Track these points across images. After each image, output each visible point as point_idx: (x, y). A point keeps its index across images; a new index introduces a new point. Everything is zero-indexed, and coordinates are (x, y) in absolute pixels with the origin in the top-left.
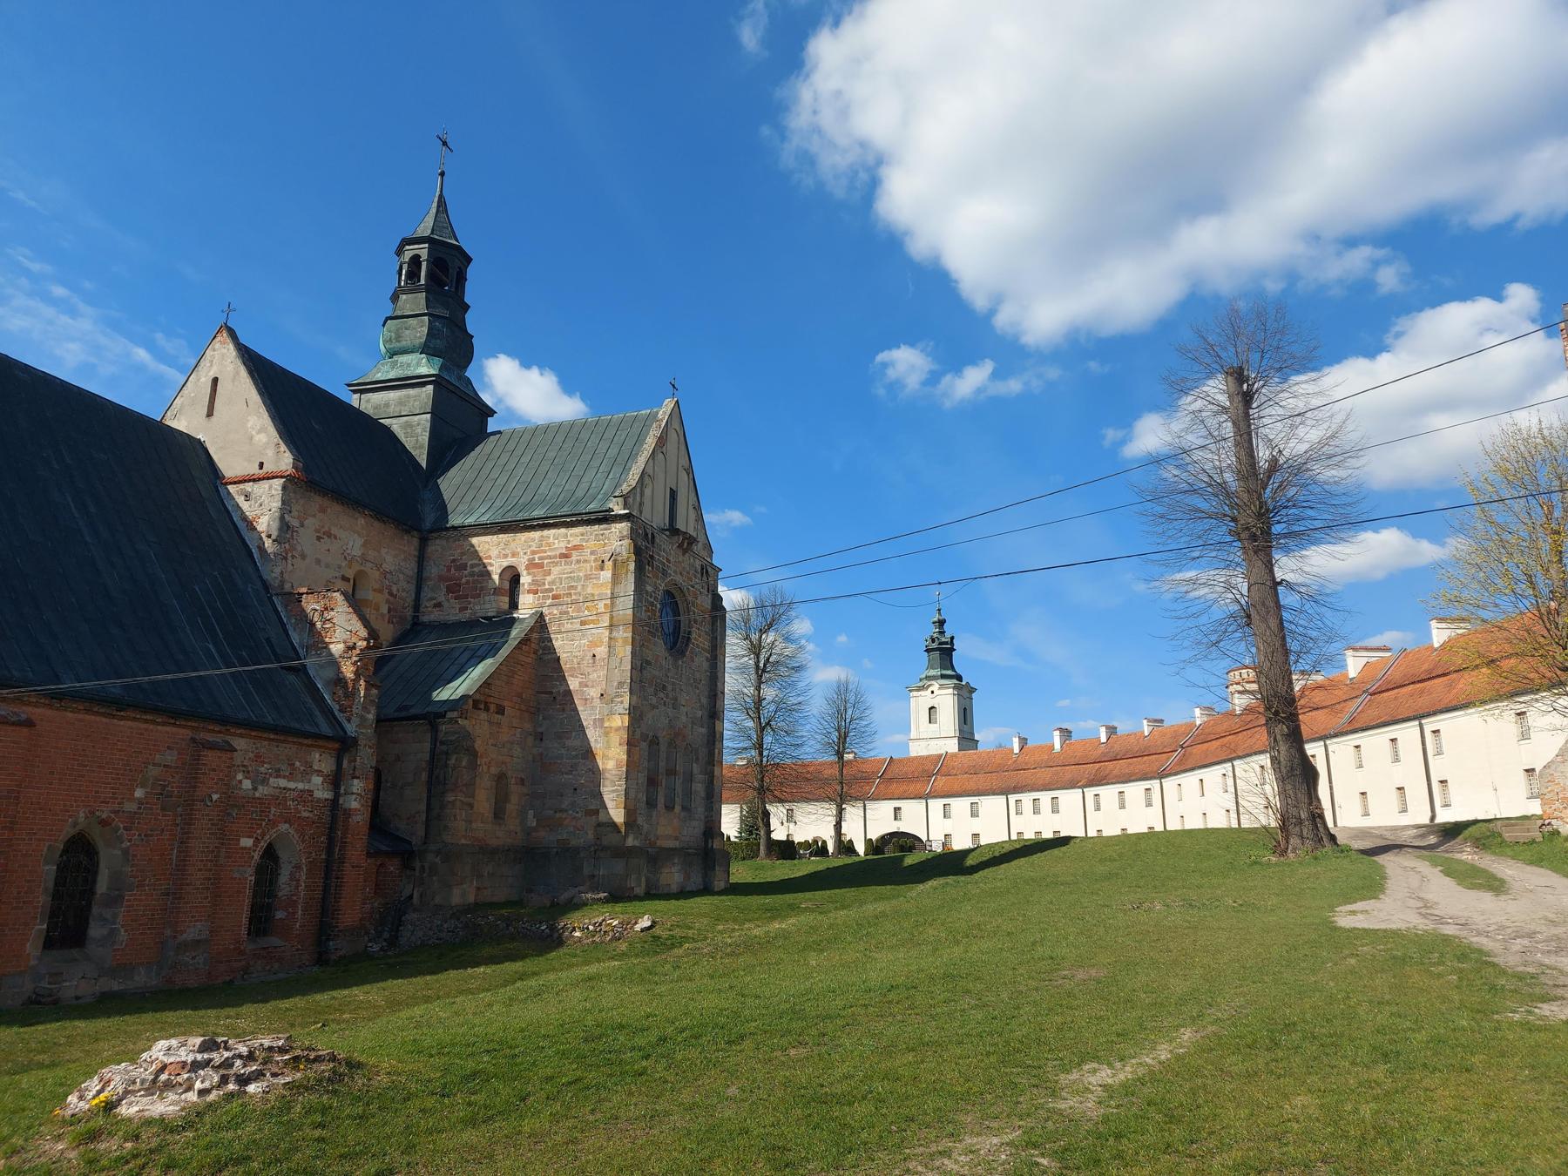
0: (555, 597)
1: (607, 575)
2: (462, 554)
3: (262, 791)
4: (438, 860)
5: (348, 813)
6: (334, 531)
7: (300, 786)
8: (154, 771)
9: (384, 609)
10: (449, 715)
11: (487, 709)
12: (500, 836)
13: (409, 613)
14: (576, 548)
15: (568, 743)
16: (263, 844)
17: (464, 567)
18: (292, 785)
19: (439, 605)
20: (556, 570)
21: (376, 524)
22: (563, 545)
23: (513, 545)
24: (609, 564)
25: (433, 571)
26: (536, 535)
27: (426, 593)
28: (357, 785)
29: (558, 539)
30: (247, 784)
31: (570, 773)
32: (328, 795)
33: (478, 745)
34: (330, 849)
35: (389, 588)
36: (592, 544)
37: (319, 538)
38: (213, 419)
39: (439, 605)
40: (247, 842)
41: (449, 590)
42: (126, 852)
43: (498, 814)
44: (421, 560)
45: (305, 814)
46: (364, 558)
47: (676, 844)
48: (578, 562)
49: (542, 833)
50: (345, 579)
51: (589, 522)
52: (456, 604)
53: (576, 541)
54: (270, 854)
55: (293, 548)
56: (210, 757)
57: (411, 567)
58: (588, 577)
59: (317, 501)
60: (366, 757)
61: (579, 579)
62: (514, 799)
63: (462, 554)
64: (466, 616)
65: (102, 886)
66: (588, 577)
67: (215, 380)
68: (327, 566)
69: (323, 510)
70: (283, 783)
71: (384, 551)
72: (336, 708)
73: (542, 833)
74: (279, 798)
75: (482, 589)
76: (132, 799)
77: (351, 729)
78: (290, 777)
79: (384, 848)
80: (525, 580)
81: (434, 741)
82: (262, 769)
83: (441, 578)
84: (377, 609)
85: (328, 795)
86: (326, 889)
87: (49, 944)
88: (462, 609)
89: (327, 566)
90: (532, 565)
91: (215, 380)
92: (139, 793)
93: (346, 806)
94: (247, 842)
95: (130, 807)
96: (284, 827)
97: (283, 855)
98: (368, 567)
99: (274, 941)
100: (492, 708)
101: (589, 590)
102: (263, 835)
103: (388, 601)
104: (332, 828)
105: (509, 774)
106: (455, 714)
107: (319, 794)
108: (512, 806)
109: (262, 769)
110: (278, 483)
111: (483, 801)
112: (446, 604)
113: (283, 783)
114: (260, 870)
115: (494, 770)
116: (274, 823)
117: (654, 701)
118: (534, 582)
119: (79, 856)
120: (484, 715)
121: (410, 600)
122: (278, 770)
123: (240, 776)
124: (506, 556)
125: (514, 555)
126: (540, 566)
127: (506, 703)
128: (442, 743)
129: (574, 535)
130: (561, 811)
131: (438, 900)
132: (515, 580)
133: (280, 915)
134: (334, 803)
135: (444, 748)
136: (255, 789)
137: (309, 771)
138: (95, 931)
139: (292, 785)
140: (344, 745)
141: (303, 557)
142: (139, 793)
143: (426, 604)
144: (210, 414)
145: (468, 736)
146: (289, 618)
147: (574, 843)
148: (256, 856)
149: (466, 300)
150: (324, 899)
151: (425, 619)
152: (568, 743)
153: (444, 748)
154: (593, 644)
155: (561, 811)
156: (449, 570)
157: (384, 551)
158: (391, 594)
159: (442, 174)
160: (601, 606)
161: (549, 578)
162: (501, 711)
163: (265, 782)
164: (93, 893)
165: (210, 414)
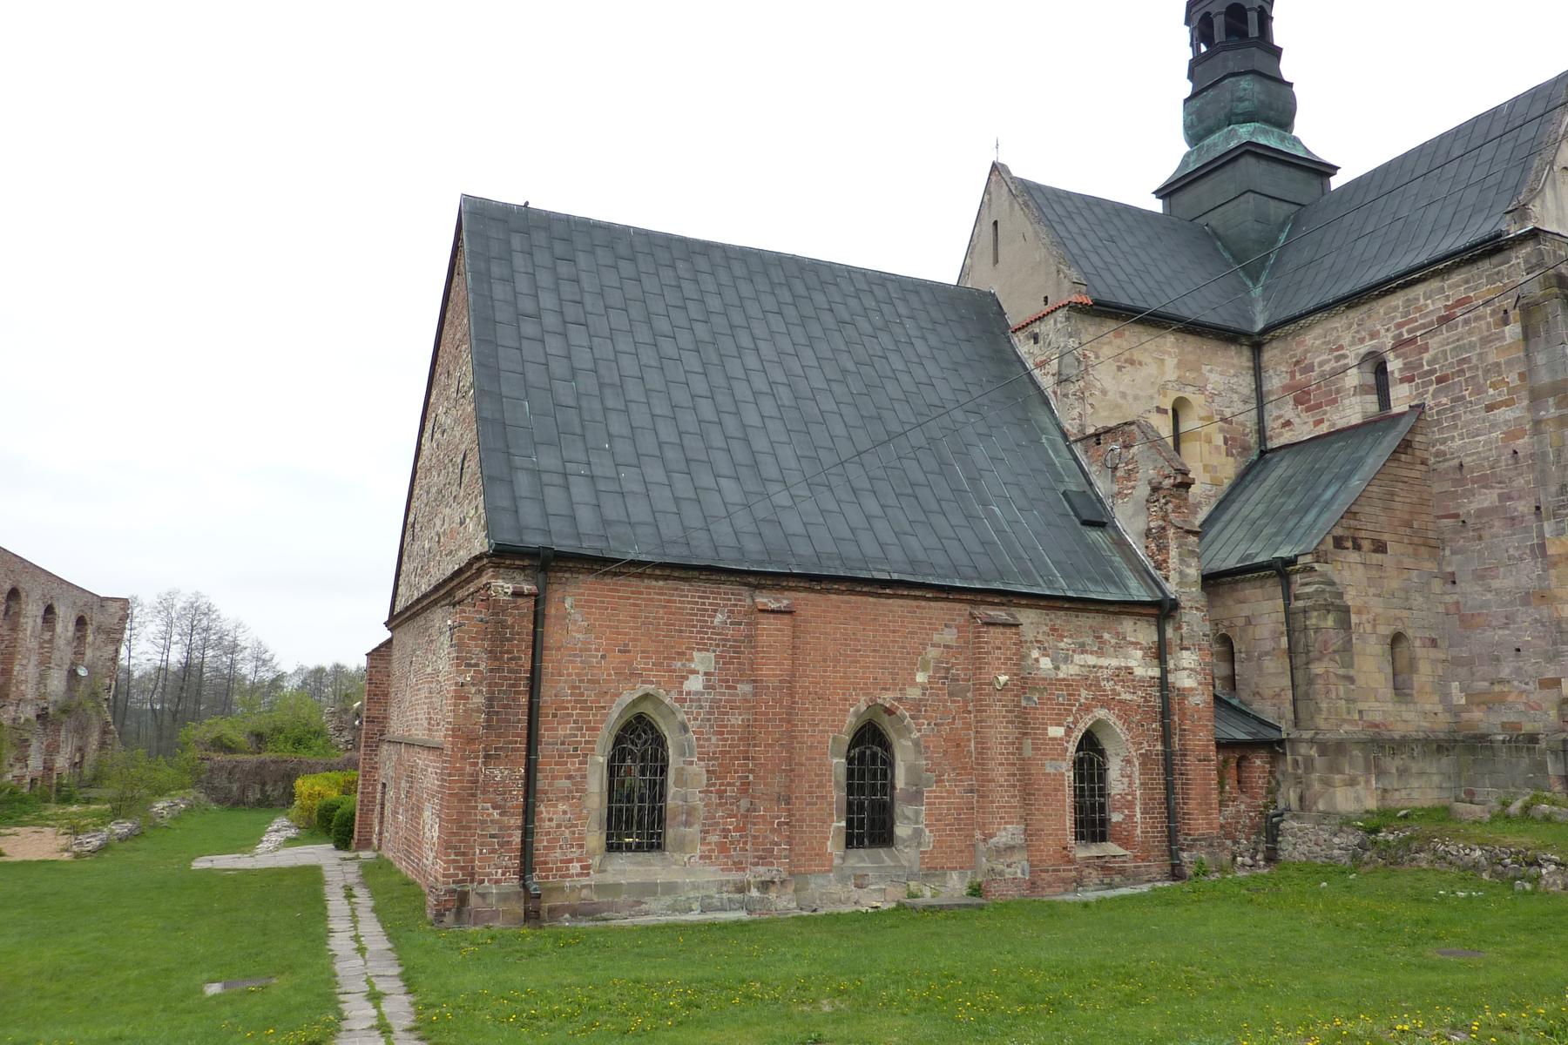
0: (1440, 380)
1: (1513, 331)
2: (1307, 351)
3: (1066, 671)
4: (1314, 752)
5: (1183, 694)
6: (1137, 355)
7: (1114, 662)
8: (932, 653)
9: (1219, 440)
10: (1301, 560)
11: (1357, 547)
12: (1410, 720)
13: (1253, 440)
14: (1459, 303)
15: (1496, 584)
16: (1078, 734)
17: (1310, 368)
18: (1104, 662)
19: (1288, 423)
20: (1434, 343)
21: (1190, 338)
22: (1440, 304)
23: (1368, 324)
24: (1514, 314)
25: (1275, 382)
26: (1398, 300)
27: (1271, 411)
28: (1188, 659)
29: (1430, 299)
30: (1046, 663)
31: (1506, 626)
33: (1350, 599)
34: (1166, 738)
35: (1220, 413)
36: (1485, 289)
37: (1120, 368)
38: (999, 266)
39: (1288, 423)
40: (1056, 732)
41: (1298, 401)
42: (916, 743)
43: (1401, 689)
44: (1258, 371)
45: (1128, 697)
46: (1179, 379)
48: (1466, 322)
49: (1477, 714)
50: (1160, 410)
51: (1473, 261)
52: (1309, 418)
53: (1461, 293)
54: (1091, 744)
55: (1088, 386)
56: (994, 636)
57: (1246, 383)
58: (1485, 341)
61: (1472, 346)
62: (1424, 668)
63: (1307, 351)
64: (1324, 429)
65: (901, 780)
66: (1485, 341)
67: (996, 223)
69: (1118, 334)
70: (1092, 660)
71: (1205, 369)
72: (1151, 566)
73: (1477, 714)
74: (1090, 679)
75: (1338, 391)
76: (914, 684)
77: (1171, 588)
78: (1100, 653)
79: (1241, 736)
80: (1394, 365)
81: (1287, 597)
82: (1062, 645)
83: (1286, 388)
84: (1210, 442)
85: (1156, 672)
86: (1169, 787)
87: (853, 840)
88: (1318, 423)
90: (1399, 344)
91: (996, 223)
92: (921, 678)
93: (1178, 684)
94: (1056, 732)
95: (913, 693)
96: (1101, 713)
97: (1109, 746)
98: (1188, 393)
99: (1111, 848)
100: (1366, 545)
101: (1492, 357)
102: (1075, 723)
103: (1221, 430)
104: (1165, 713)
105: (1410, 633)
106: (1309, 559)
107: (1139, 672)
108: (1425, 674)
109: (1062, 645)
110: (1060, 314)
111: (1371, 666)
112: (1296, 421)
113: (1092, 660)
114: (1078, 764)
115: (1385, 630)
116: (1087, 709)
118: (1407, 367)
119: (870, 746)
120: (1353, 556)
121: (1251, 425)
122: (1083, 645)
123: (1035, 654)
124: (1362, 340)
125: (1374, 335)
126: (1412, 340)
127: (1385, 537)
128: (1297, 598)
129: (1454, 286)
130: (1501, 681)
131: (1321, 806)
132: (1381, 370)
133: (1116, 817)
134: (1163, 683)
135: (1300, 604)
136: (1057, 668)
137: (1122, 644)
138: (901, 830)
139: (1104, 662)
140: (1163, 611)
141: (1104, 392)
142: (921, 678)
143: (1272, 425)
144: (996, 261)
146: (1090, 464)
147: (1528, 727)
148: (1072, 748)
149: (1277, 42)
150: (1167, 799)
151: (1272, 444)
152: (1496, 584)
153: (1300, 604)
154: (1511, 436)
155: (1501, 681)
156: (1293, 374)
157: (1205, 369)
158: (1224, 420)
160: (1512, 378)
161: (1426, 356)
162: (1380, 547)
163: (1066, 659)
164: (893, 787)
165: (996, 261)
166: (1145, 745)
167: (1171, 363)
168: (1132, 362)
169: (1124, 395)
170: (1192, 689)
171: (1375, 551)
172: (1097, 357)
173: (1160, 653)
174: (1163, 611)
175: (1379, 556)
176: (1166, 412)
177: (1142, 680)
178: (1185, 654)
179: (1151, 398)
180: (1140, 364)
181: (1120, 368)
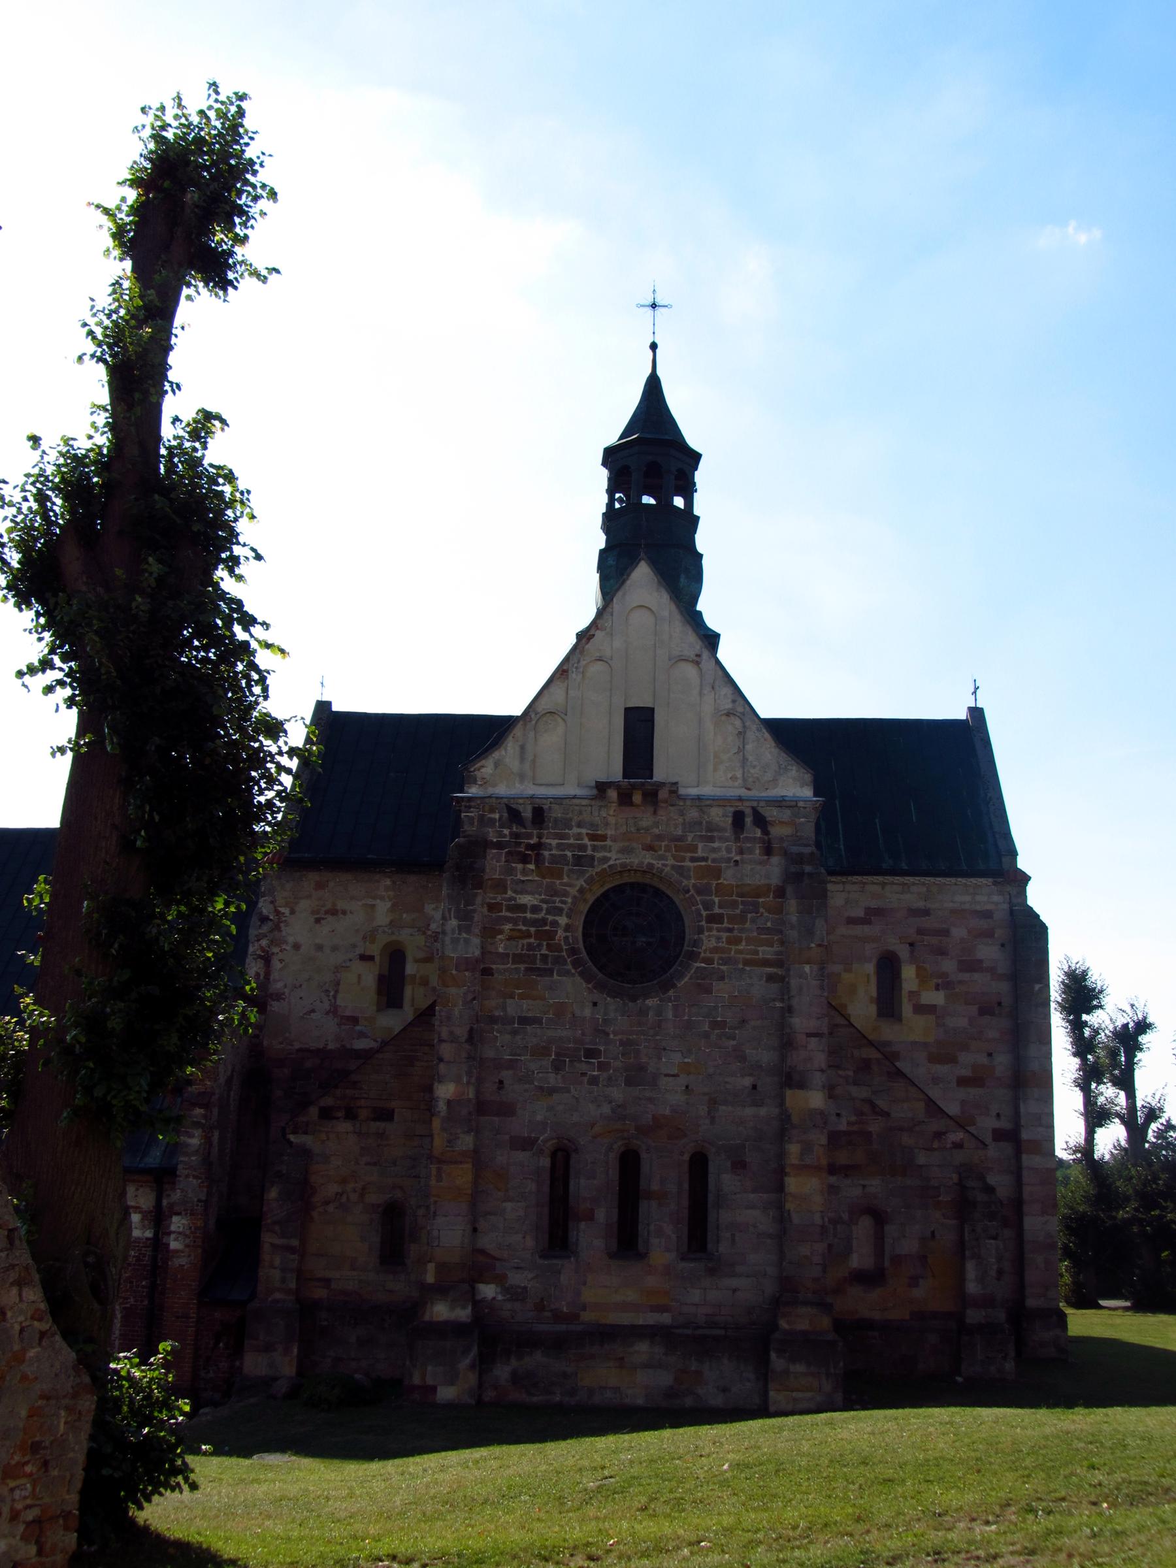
6: (341, 905)
11: (351, 1115)
32: (149, 1234)
37: (318, 921)
47: (666, 1318)
59: (313, 877)
60: (189, 1186)
68: (335, 949)
69: (320, 886)
89: (335, 949)
117: (553, 1079)
120: (344, 1126)
134: (158, 1244)
141: (297, 947)
145: (305, 1153)
159: (654, 347)
162: (386, 1115)
166: (132, 1300)
167: (383, 908)
168: (333, 912)
169: (320, 948)
170: (177, 1251)
171: (376, 1119)
172: (293, 912)
173: (158, 1218)
174: (162, 1178)
175: (381, 1125)
176: (371, 958)
177: (138, 1240)
178: (175, 1219)
179: (354, 946)
180: (344, 912)
181: (318, 921)
